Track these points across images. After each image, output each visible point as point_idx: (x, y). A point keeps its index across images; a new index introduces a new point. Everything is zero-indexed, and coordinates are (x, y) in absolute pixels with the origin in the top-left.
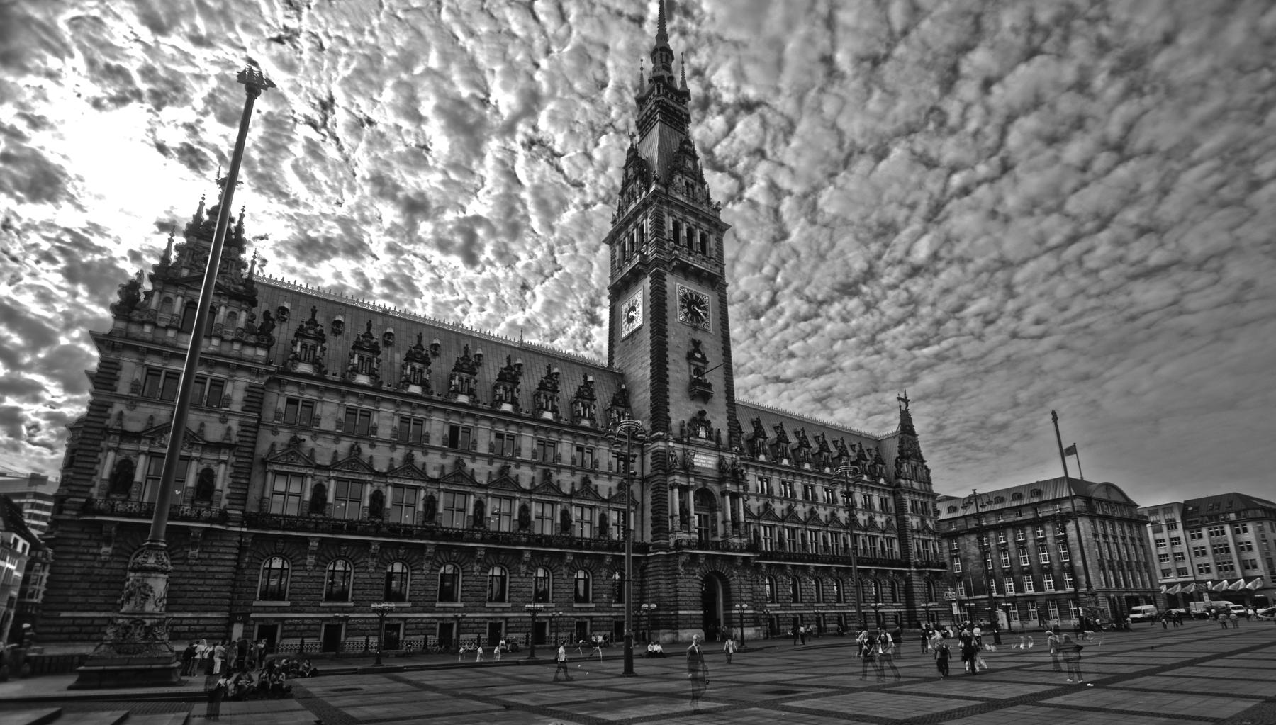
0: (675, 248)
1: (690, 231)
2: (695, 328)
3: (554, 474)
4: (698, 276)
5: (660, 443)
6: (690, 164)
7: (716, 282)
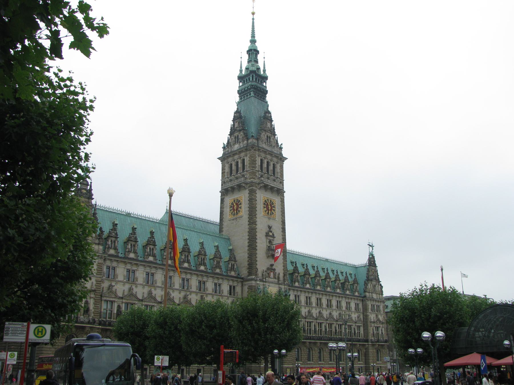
0: (262, 176)
2: (269, 218)
3: (206, 298)
4: (272, 189)
5: (253, 282)
6: (269, 124)
7: (280, 192)
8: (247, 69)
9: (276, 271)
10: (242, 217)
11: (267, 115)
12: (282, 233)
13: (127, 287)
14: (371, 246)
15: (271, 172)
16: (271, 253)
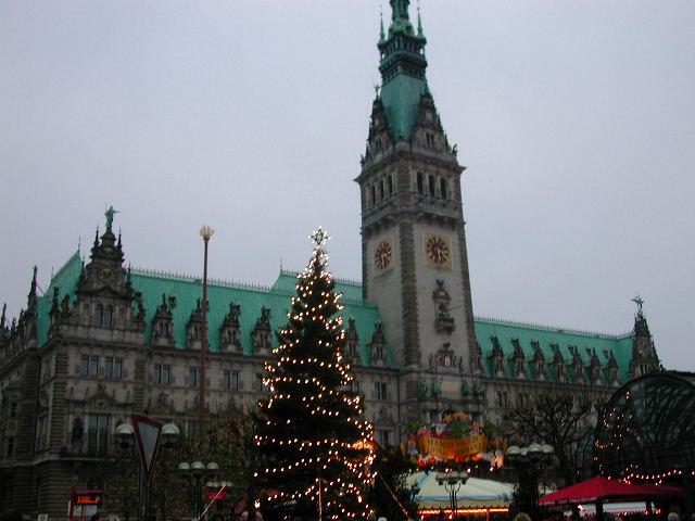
0: (420, 200)
1: (432, 180)
2: (438, 268)
4: (441, 221)
5: (414, 375)
6: (429, 116)
7: (456, 224)
8: (390, 30)
9: (455, 354)
10: (391, 270)
11: (425, 100)
14: (640, 302)
15: (438, 193)
16: (445, 325)
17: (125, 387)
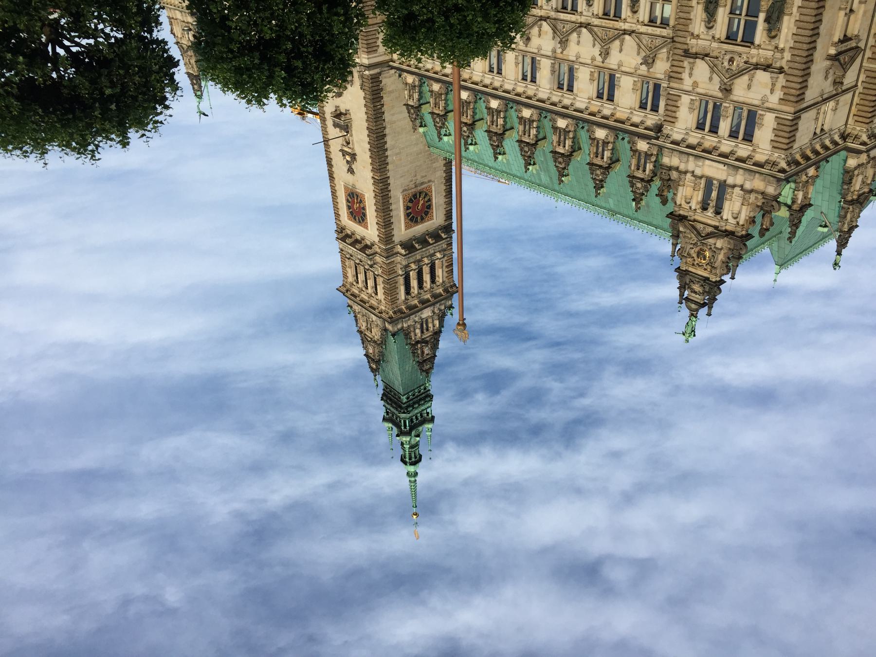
0: (371, 266)
2: (354, 186)
11: (374, 366)
12: (332, 156)
13: (613, 61)
17: (695, 84)
